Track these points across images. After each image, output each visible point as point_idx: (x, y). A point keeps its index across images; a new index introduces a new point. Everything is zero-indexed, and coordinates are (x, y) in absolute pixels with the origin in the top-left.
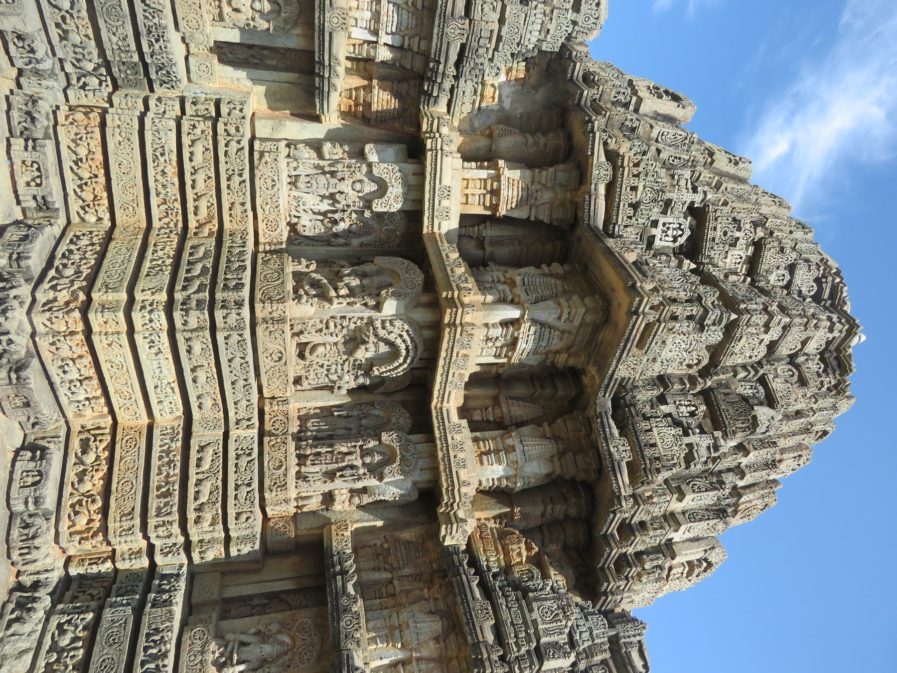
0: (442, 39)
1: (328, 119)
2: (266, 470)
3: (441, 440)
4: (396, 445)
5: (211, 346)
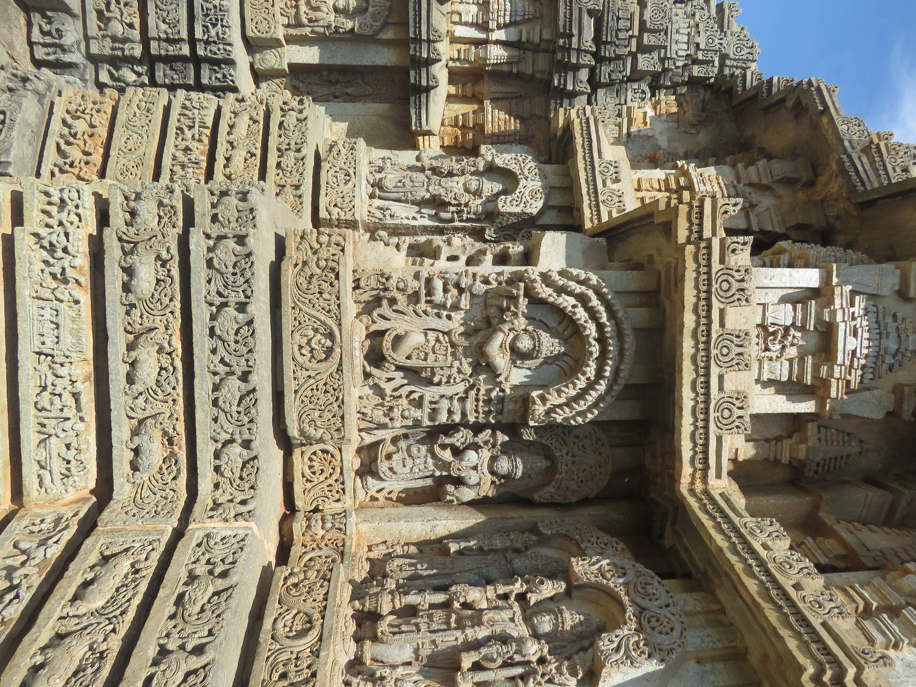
0: (571, 6)
1: (427, 144)
2: (265, 636)
3: (736, 552)
4: (616, 584)
5: (175, 273)
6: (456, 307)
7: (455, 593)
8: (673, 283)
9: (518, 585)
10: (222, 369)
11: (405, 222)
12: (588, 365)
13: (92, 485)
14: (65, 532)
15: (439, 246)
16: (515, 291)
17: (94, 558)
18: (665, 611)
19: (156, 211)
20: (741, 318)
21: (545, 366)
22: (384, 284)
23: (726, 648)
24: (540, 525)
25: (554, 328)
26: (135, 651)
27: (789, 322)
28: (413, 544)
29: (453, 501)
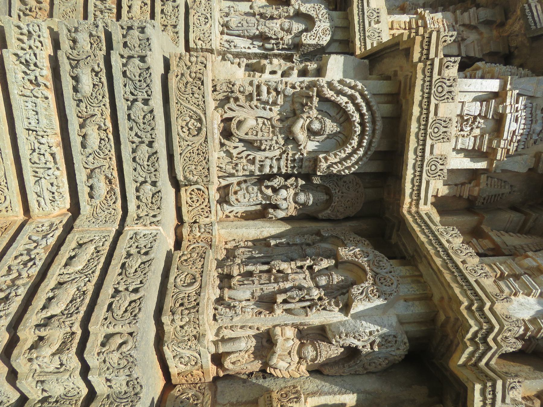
3: (431, 244)
4: (363, 261)
5: (104, 80)
6: (275, 103)
7: (273, 265)
8: (408, 88)
9: (308, 261)
10: (136, 140)
11: (243, 50)
12: (353, 139)
13: (68, 206)
14: (56, 231)
15: (264, 65)
16: (311, 93)
17: (74, 245)
18: (389, 275)
19: (88, 39)
20: (448, 110)
21: (328, 140)
22: (231, 88)
23: (421, 294)
24: (322, 231)
25: (334, 116)
26: (102, 290)
27: (477, 113)
28: (250, 241)
29: (272, 218)
